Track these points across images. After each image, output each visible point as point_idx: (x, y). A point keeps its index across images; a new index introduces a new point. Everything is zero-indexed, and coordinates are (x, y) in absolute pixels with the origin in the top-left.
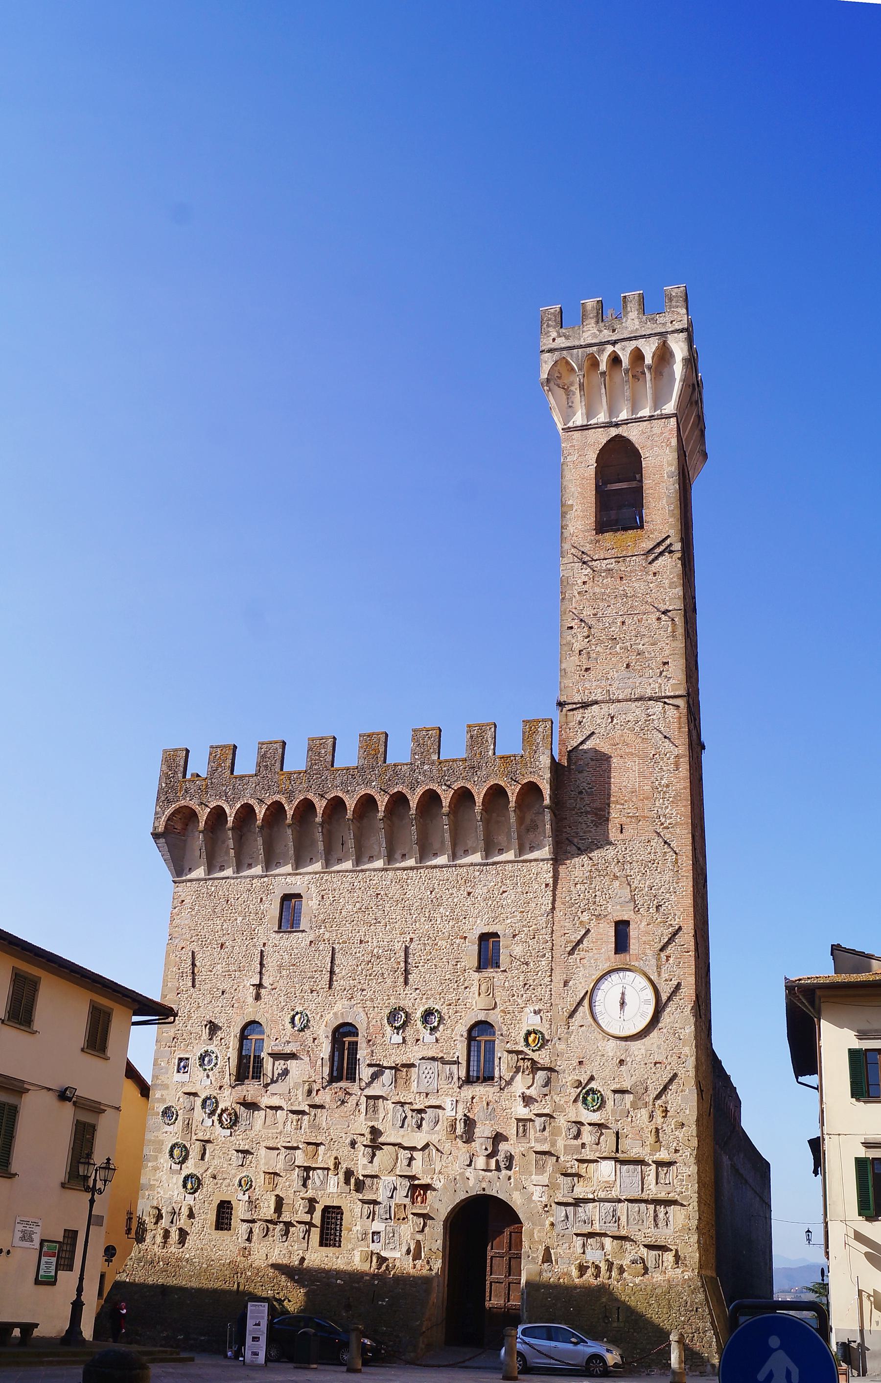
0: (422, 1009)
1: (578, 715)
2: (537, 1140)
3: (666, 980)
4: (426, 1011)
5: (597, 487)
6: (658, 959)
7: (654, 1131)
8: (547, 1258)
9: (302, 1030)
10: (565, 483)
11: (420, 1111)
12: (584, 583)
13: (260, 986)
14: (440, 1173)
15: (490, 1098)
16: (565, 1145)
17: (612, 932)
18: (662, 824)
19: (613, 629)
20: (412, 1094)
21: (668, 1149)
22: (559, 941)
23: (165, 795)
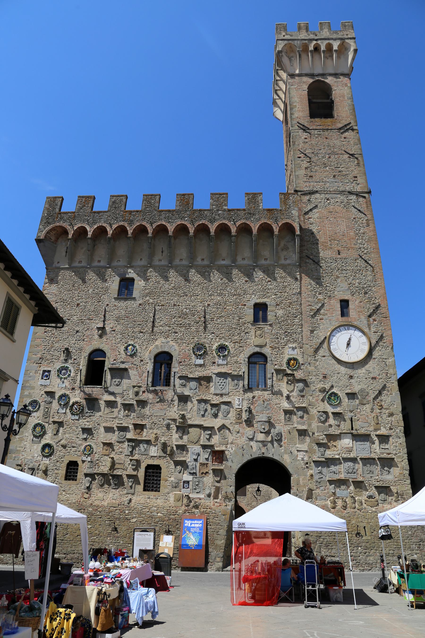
0: (217, 344)
1: (307, 197)
2: (298, 423)
3: (374, 332)
4: (219, 346)
5: (309, 100)
6: (368, 321)
7: (375, 417)
9: (131, 356)
10: (291, 96)
12: (306, 138)
13: (103, 329)
14: (232, 443)
15: (265, 398)
16: (318, 426)
17: (339, 306)
18: (363, 252)
19: (324, 160)
20: (211, 393)
22: (305, 308)
23: (47, 219)
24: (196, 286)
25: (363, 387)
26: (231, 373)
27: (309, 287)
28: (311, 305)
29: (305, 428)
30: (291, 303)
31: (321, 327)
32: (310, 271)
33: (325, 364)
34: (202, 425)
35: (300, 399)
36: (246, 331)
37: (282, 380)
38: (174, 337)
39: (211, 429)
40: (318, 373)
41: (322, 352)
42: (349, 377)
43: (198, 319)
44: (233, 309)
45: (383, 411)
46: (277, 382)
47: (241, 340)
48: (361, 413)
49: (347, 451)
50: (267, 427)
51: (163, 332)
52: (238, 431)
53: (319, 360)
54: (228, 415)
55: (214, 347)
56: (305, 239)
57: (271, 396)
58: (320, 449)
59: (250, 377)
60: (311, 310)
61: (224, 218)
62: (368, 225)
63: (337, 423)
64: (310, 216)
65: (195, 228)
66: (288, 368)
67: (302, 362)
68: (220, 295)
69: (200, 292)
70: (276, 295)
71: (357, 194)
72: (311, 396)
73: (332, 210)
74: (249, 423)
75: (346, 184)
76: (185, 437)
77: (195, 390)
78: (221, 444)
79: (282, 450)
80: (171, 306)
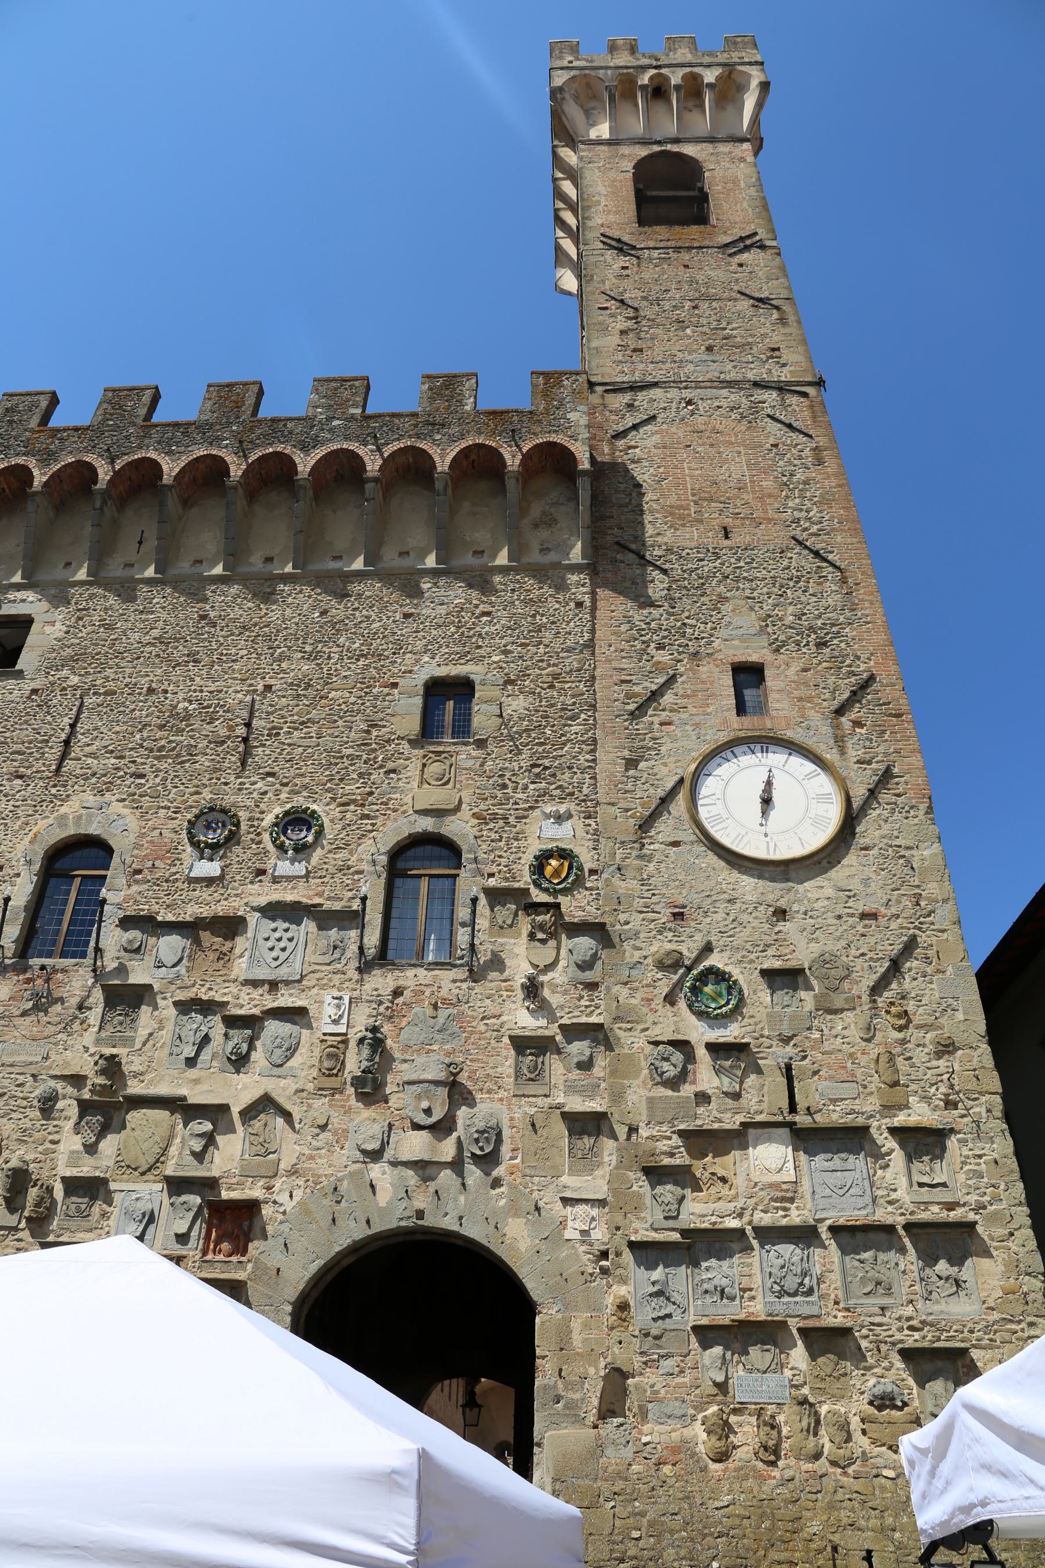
0: (278, 810)
1: (627, 398)
2: (571, 1089)
3: (858, 762)
4: (287, 813)
6: (837, 727)
8: (614, 1401)
11: (251, 1023)
14: (293, 1172)
15: (444, 993)
16: (651, 1101)
21: (926, 1099)
22: (606, 691)
24: (232, 635)
25: (827, 949)
26: (321, 905)
27: (624, 628)
28: (630, 681)
29: (599, 1109)
30: (556, 676)
31: (663, 749)
32: (628, 584)
33: (678, 870)
34: (184, 1098)
35: (581, 997)
36: (390, 765)
37: (511, 926)
38: (132, 790)
39: (217, 1113)
40: (655, 899)
41: (669, 829)
42: (774, 913)
43: (223, 732)
44: (352, 699)
45: (914, 1034)
46: (491, 935)
47: (371, 793)
48: (826, 1046)
49: (773, 1200)
50: (443, 1104)
51: (94, 774)
52: (322, 1121)
53: (658, 856)
54: (288, 1059)
55: (269, 819)
56: (614, 500)
57: (465, 985)
58: (659, 1189)
59: (394, 923)
60: (629, 696)
61: (347, 438)
62: (820, 462)
63: (727, 1084)
64: (633, 443)
65: (249, 466)
66: (537, 885)
67: (594, 865)
68: (310, 657)
69: (245, 652)
70: (506, 652)
71: (781, 388)
72: (626, 984)
73: (703, 428)
74: (370, 1089)
75: (745, 365)
76: (109, 1144)
77: (174, 966)
78: (248, 1174)
79: (500, 1198)
80: (140, 694)
